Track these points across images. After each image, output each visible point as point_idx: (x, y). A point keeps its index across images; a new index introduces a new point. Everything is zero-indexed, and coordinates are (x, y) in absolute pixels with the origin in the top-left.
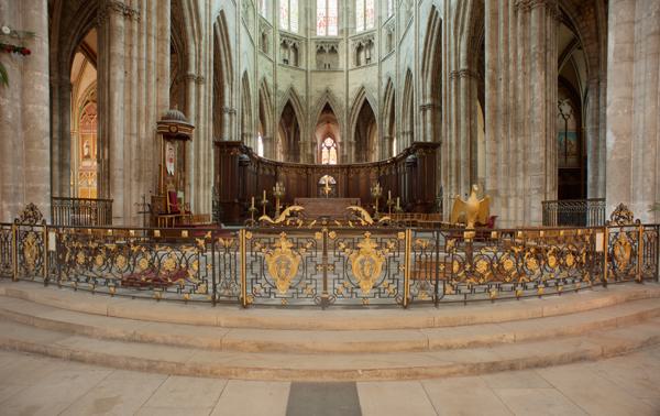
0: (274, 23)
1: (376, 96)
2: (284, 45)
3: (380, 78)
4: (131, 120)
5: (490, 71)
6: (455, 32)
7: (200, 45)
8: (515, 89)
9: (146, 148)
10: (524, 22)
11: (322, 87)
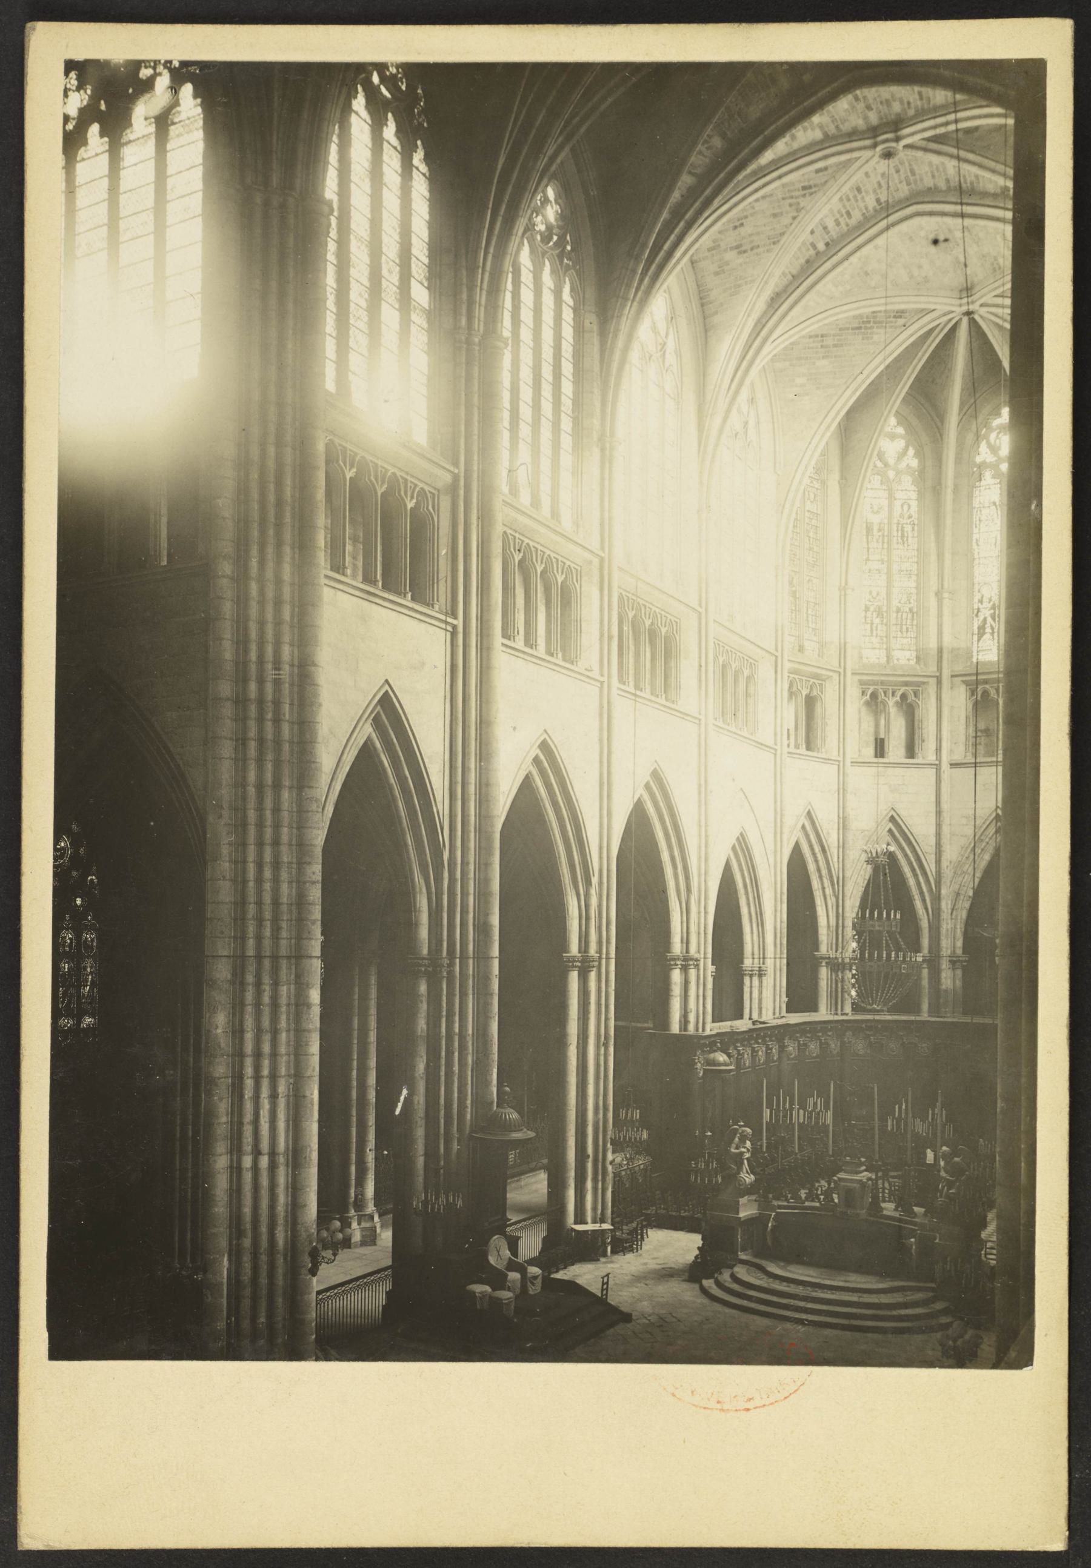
2: (874, 702)
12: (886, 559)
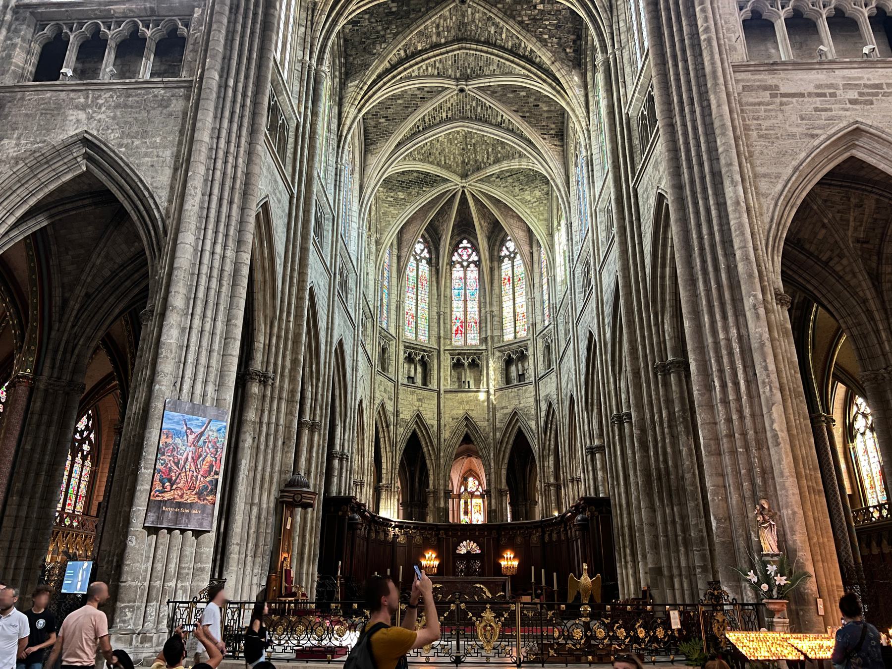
1: (533, 424)
2: (410, 359)
3: (537, 401)
4: (254, 488)
5: (638, 432)
6: (613, 370)
7: (317, 386)
8: (665, 453)
9: (267, 519)
10: (666, 384)
11: (460, 412)
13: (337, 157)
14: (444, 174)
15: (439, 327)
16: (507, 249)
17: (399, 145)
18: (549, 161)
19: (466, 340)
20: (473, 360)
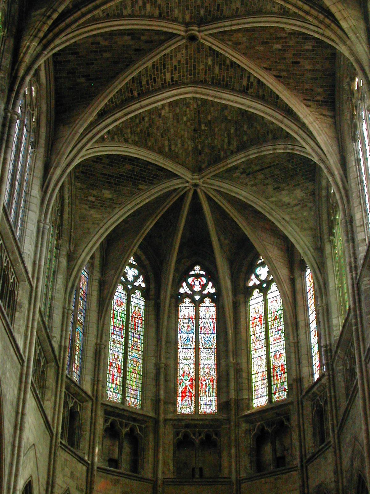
0: (96, 392)
12: (124, 336)
13: (7, 103)
14: (169, 165)
15: (157, 385)
16: (257, 276)
17: (103, 114)
18: (316, 135)
19: (197, 405)
20: (208, 436)
